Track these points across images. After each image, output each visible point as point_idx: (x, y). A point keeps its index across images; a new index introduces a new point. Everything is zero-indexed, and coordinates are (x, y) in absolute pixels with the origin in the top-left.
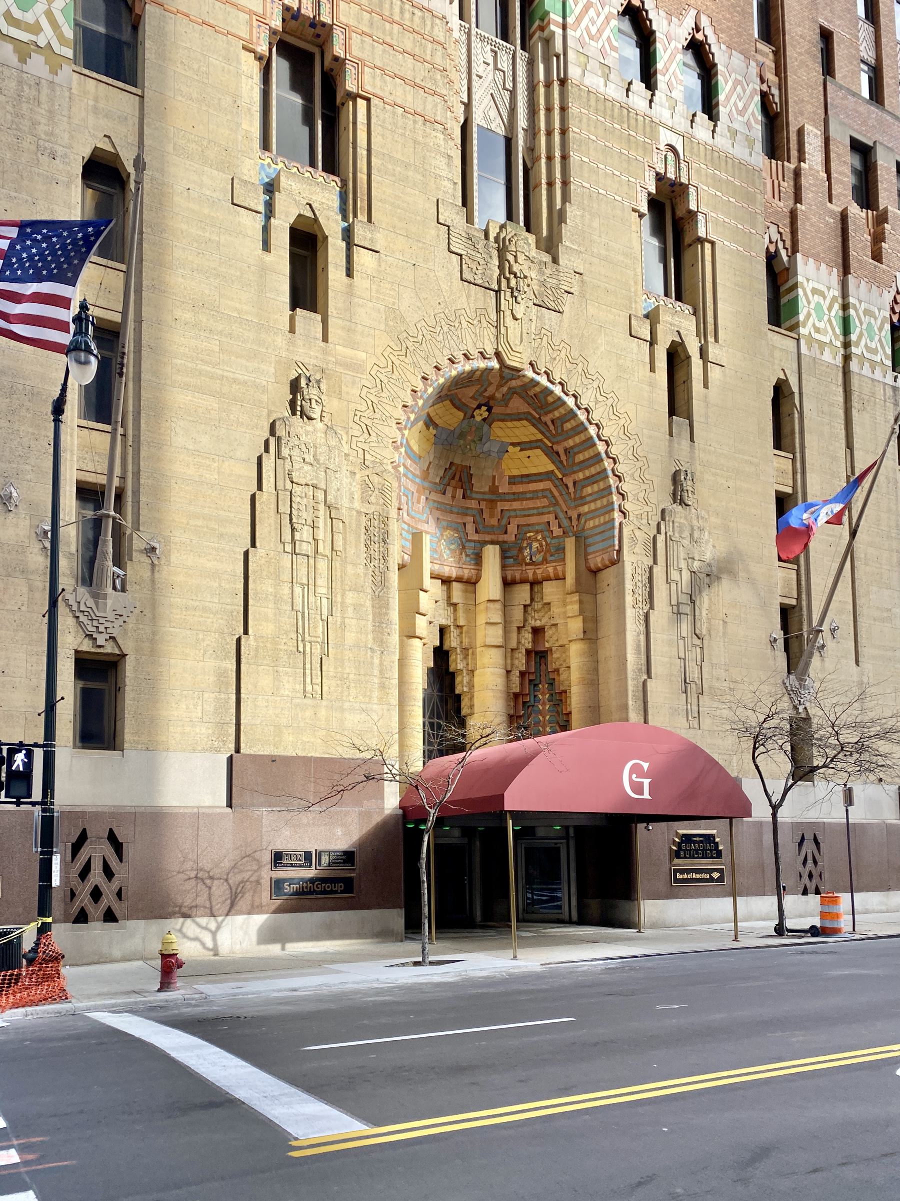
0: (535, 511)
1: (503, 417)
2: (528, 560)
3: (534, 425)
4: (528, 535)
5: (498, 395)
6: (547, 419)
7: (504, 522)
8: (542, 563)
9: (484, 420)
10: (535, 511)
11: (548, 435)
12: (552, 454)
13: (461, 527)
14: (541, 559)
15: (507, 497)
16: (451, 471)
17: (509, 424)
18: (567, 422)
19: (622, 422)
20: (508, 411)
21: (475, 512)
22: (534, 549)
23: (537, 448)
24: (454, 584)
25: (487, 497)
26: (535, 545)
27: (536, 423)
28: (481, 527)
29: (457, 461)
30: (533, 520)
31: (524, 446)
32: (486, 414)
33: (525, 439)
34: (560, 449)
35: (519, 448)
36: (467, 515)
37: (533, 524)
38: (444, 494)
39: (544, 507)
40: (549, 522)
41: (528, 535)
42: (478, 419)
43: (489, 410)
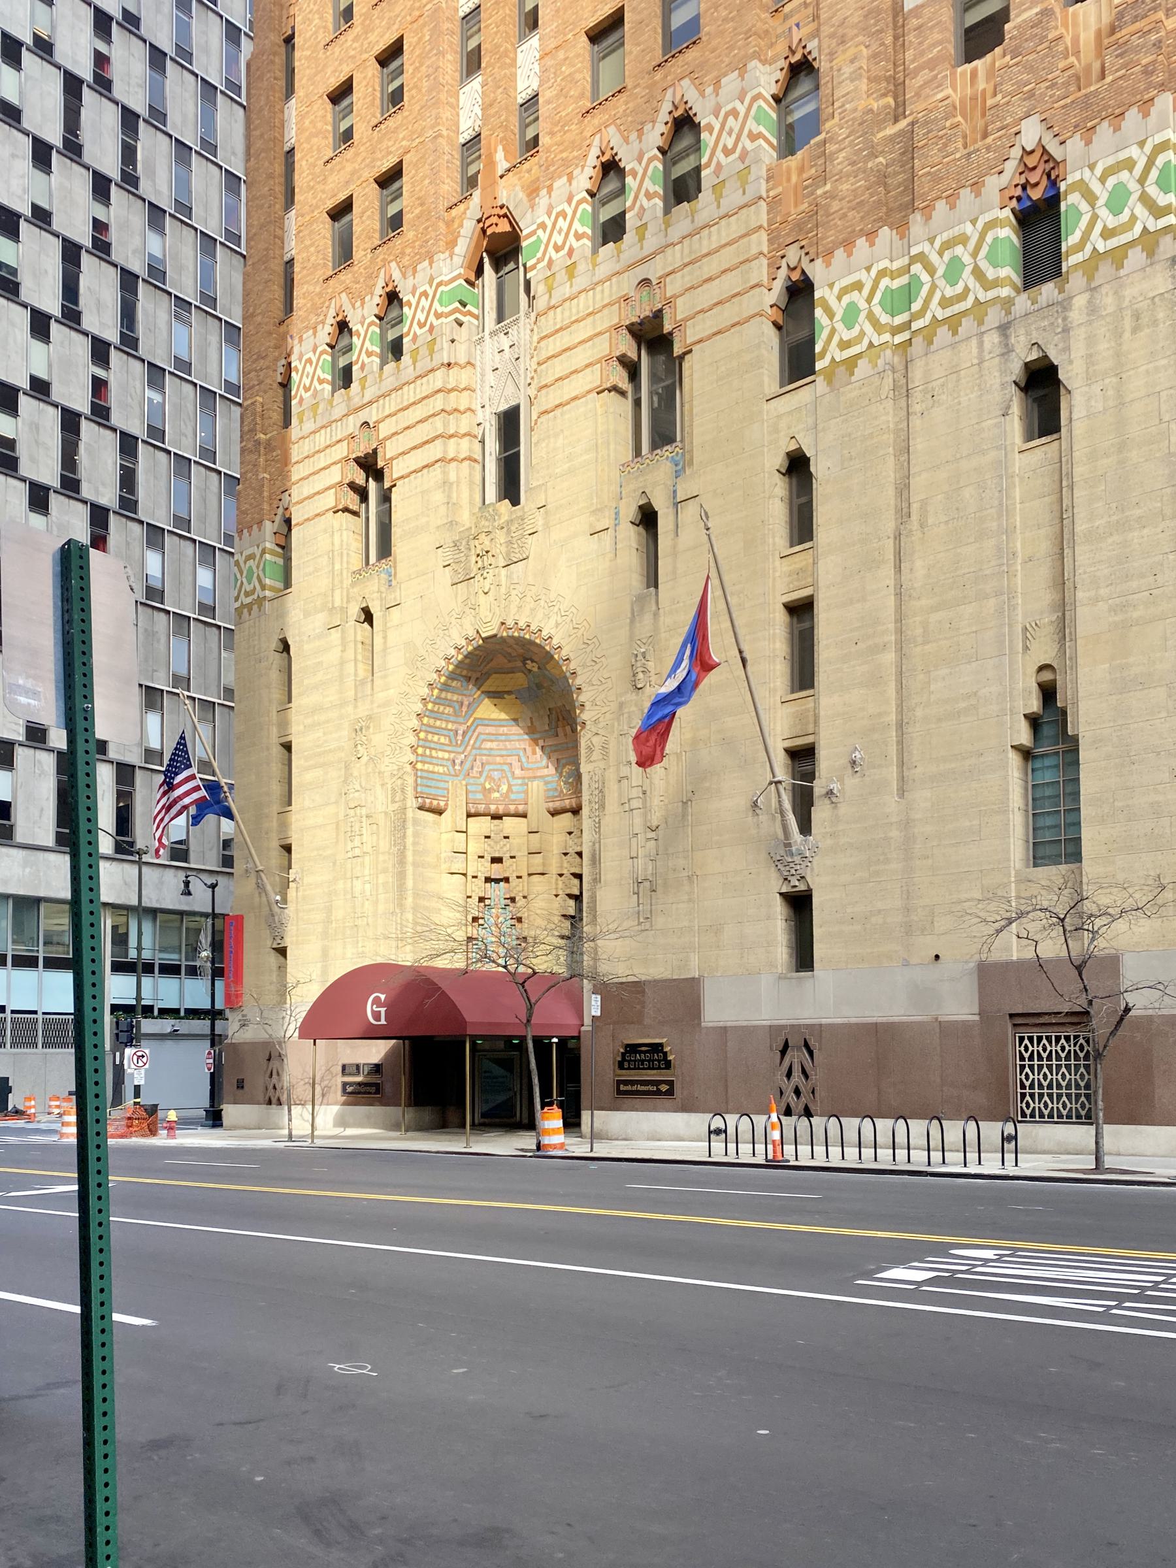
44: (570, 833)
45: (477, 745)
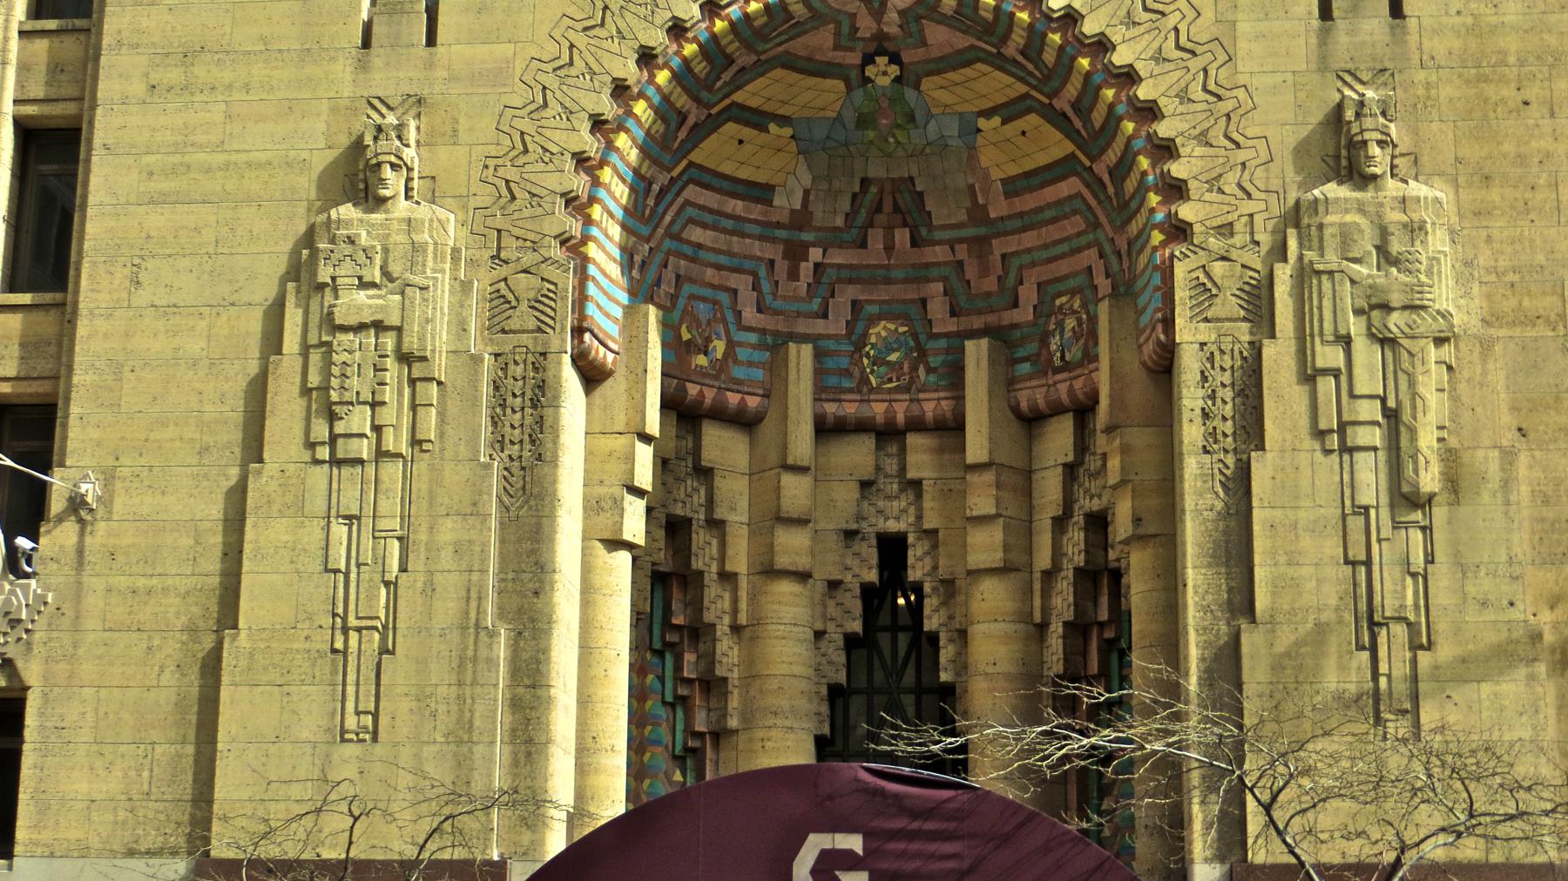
0: (1065, 248)
1: (931, 66)
2: (1057, 362)
3: (1000, 68)
4: (1058, 302)
5: (893, 30)
6: (1010, 50)
7: (1011, 280)
8: (1080, 364)
9: (898, 80)
10: (1065, 248)
11: (1035, 83)
12: (1059, 120)
13: (914, 311)
14: (1080, 354)
15: (1009, 225)
16: (869, 197)
17: (950, 75)
18: (1041, 51)
19: (1173, 20)
20: (936, 53)
21: (946, 271)
22: (1068, 334)
23: (1029, 111)
24: (912, 439)
25: (964, 233)
26: (1070, 323)
27: (1000, 62)
28: (962, 301)
29: (876, 171)
30: (1063, 267)
31: (1010, 111)
32: (894, 70)
33: (1002, 100)
34: (1062, 104)
35: (997, 120)
36: (928, 280)
37: (1066, 277)
38: (863, 245)
39: (1079, 234)
40: (1090, 269)
41: (1058, 302)
42: (884, 81)
43: (895, 59)
44: (865, 485)
45: (676, 228)
